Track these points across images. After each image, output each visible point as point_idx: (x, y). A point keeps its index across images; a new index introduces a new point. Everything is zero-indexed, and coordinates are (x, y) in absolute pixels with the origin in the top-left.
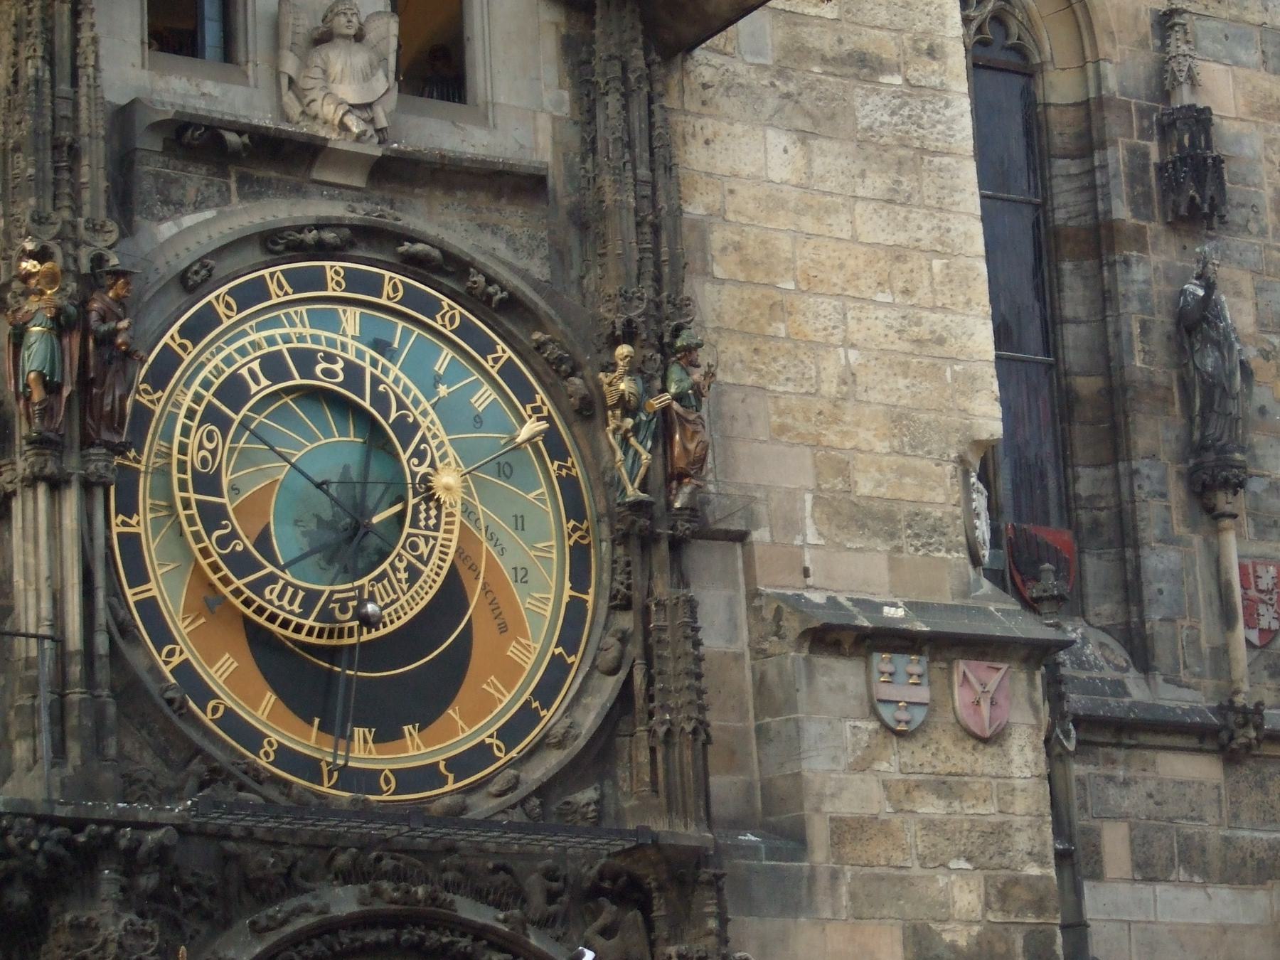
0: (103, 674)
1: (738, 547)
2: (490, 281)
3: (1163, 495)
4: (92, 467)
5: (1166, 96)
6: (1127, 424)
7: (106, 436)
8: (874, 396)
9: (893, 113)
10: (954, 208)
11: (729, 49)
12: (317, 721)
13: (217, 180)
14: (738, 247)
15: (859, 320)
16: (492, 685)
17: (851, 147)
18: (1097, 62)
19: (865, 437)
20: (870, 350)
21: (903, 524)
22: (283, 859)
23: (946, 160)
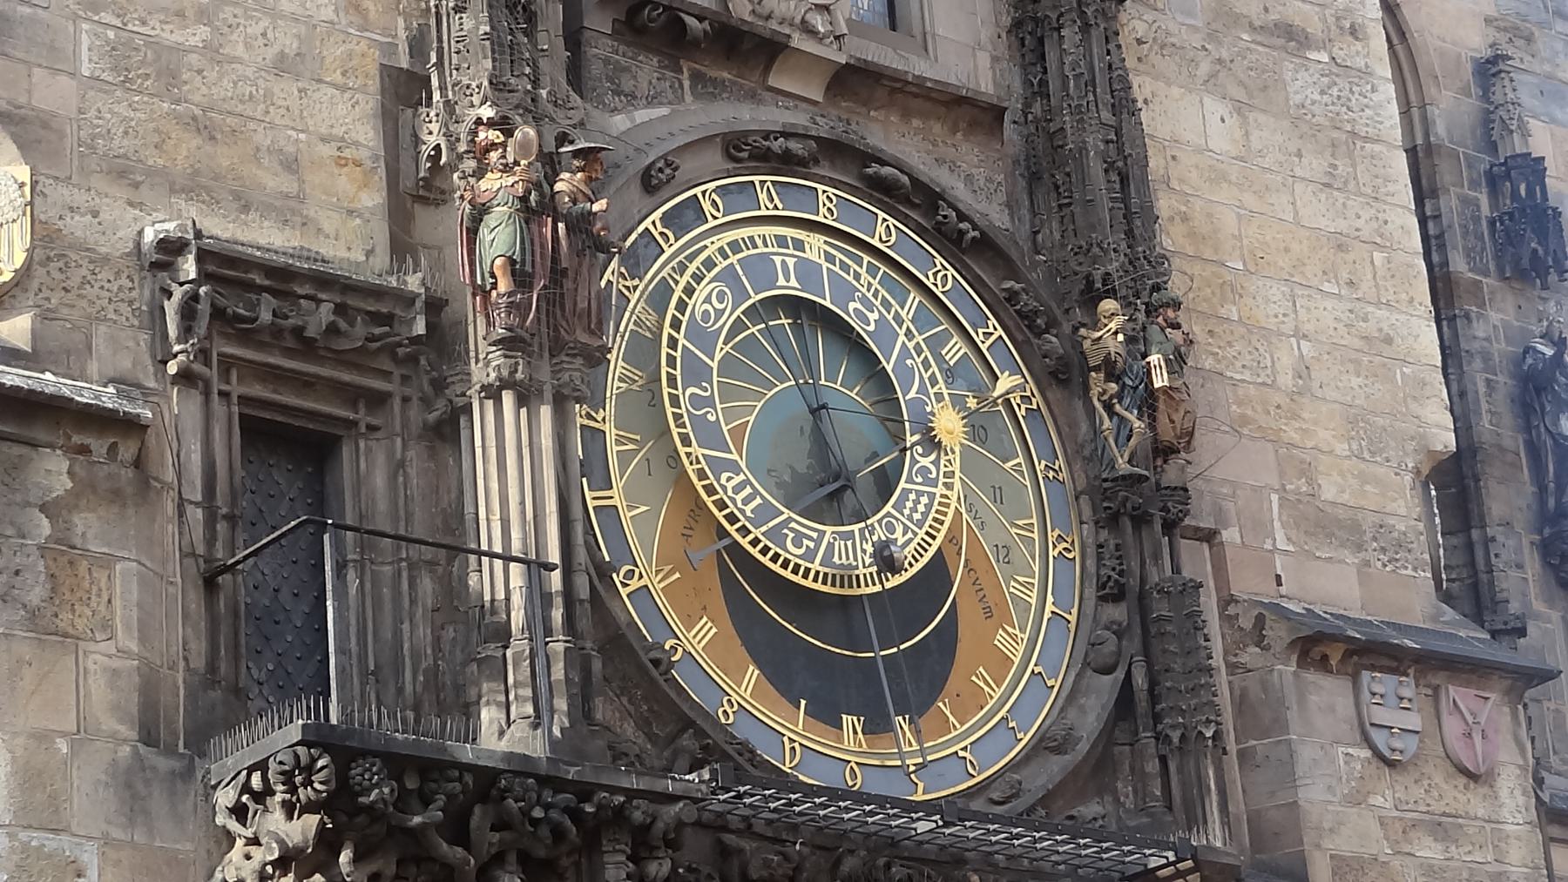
0: (584, 623)
1: (1205, 546)
2: (962, 217)
3: (1520, 566)
4: (566, 377)
5: (1493, 148)
6: (1478, 489)
7: (584, 338)
8: (1331, 394)
9: (1322, 93)
10: (1389, 199)
11: (1160, 5)
12: (803, 702)
13: (669, 74)
14: (1185, 218)
15: (1309, 309)
16: (982, 677)
17: (1286, 123)
18: (1423, 107)
19: (1323, 434)
20: (1321, 342)
21: (1369, 536)
22: (786, 857)
23: (1377, 148)
